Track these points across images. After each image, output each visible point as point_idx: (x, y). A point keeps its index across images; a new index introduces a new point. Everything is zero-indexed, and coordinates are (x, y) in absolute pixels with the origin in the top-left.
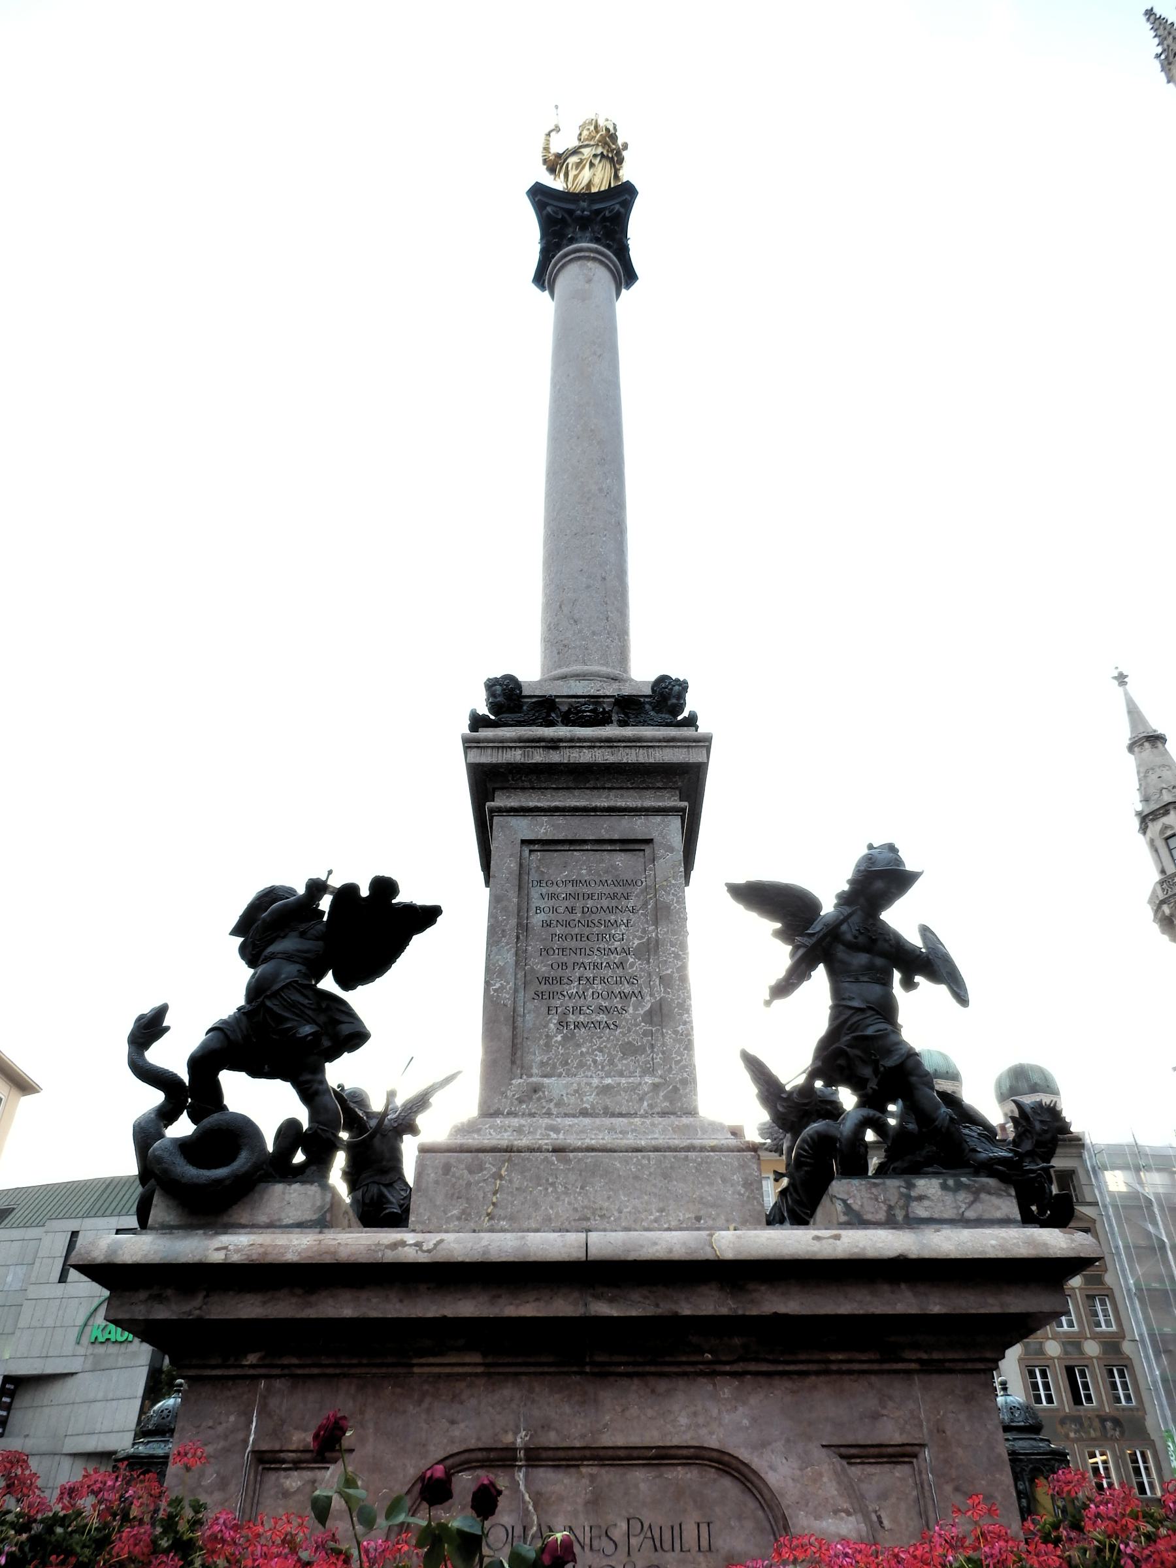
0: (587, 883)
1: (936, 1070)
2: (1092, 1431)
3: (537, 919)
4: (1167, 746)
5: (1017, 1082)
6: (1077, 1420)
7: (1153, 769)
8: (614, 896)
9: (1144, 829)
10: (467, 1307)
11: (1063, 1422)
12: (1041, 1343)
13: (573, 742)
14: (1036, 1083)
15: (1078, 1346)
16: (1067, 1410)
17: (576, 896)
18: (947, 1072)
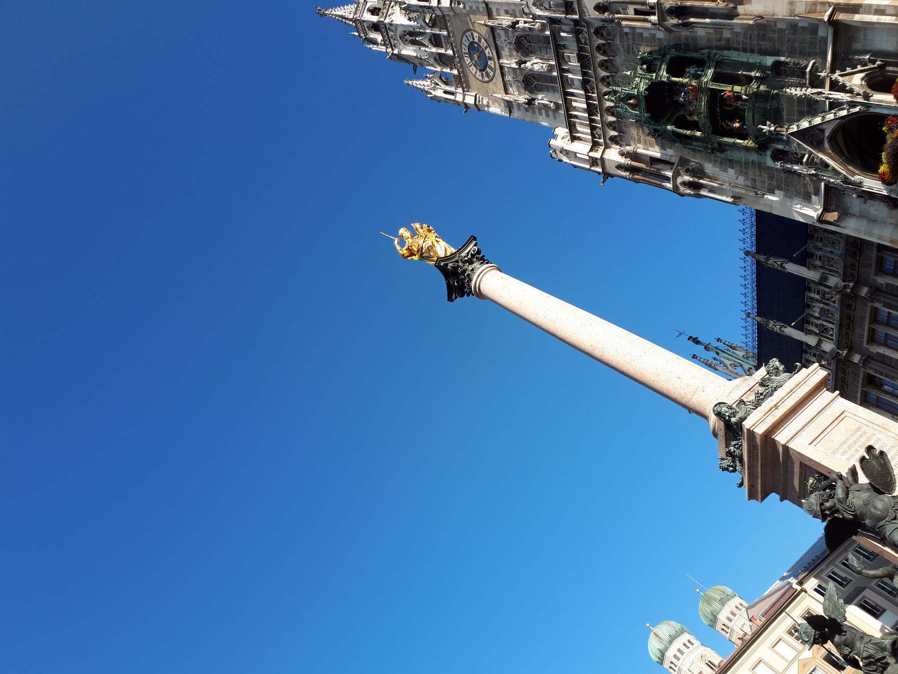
0: (847, 440)
8: (861, 436)
13: (783, 400)
17: (849, 448)
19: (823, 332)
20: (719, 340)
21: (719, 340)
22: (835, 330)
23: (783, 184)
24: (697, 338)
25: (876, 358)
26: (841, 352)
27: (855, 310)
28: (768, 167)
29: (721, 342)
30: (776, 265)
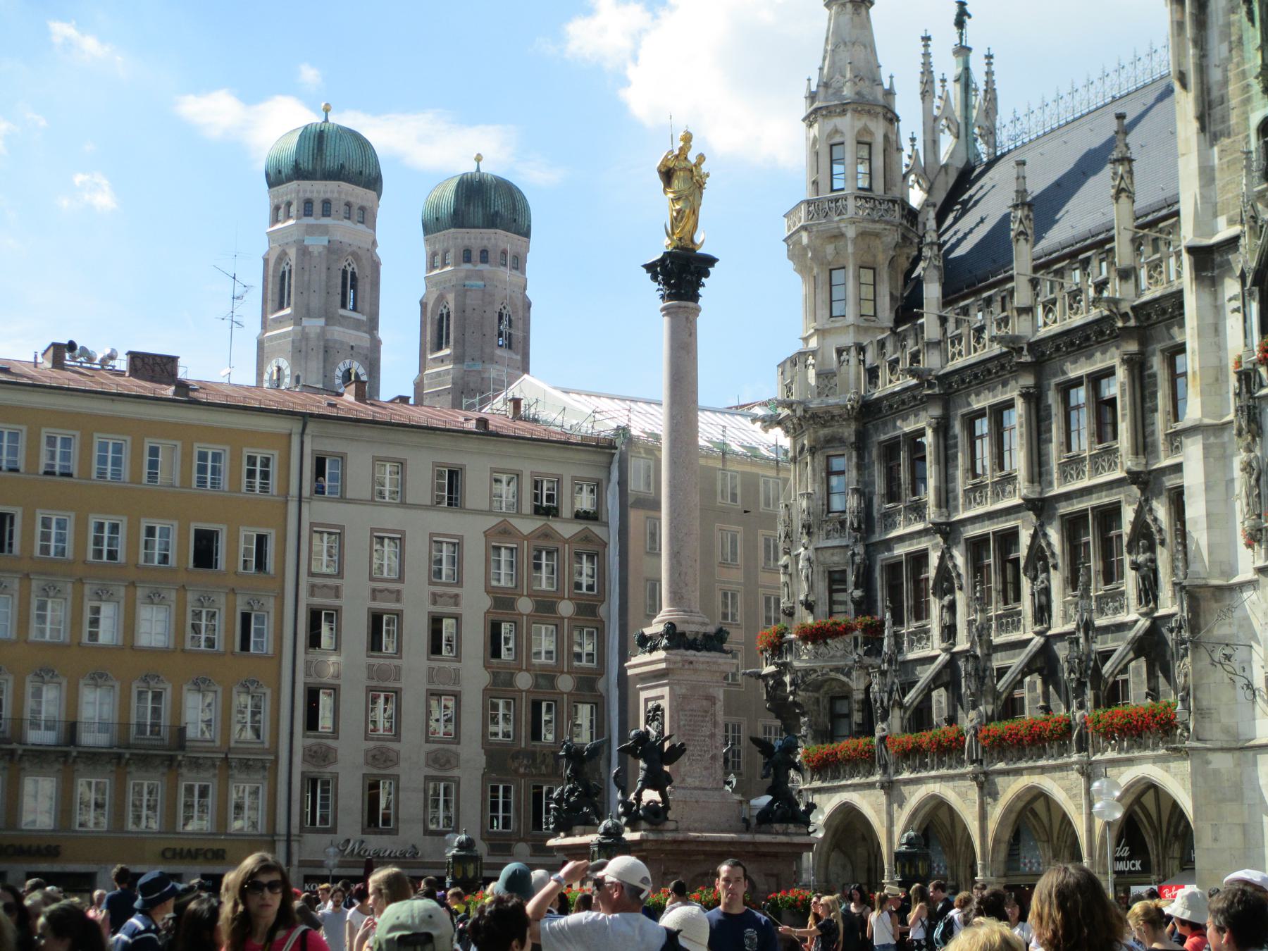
1: (342, 166)
2: (543, 768)
3: (682, 723)
4: (872, 10)
5: (468, 204)
6: (532, 755)
7: (845, 44)
9: (810, 119)
10: (707, 848)
11: (515, 756)
12: (512, 675)
14: (497, 213)
15: (551, 679)
16: (523, 745)
18: (361, 173)
19: (1044, 307)
20: (989, 57)
21: (989, 57)
22: (1055, 325)
23: (1229, 158)
24: (969, 16)
25: (1042, 406)
26: (1025, 352)
27: (1099, 343)
28: (1247, 119)
29: (987, 64)
30: (1117, 182)
